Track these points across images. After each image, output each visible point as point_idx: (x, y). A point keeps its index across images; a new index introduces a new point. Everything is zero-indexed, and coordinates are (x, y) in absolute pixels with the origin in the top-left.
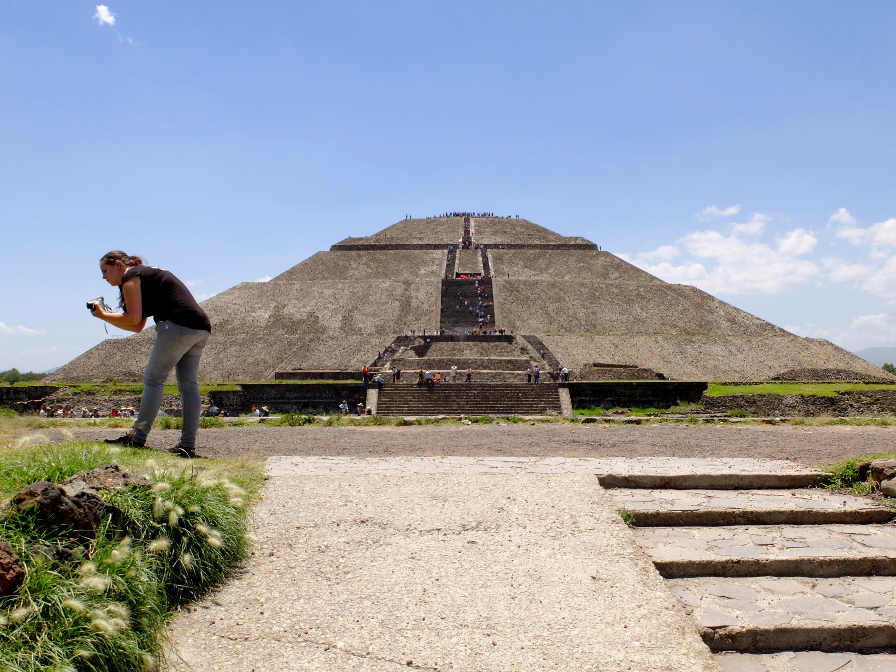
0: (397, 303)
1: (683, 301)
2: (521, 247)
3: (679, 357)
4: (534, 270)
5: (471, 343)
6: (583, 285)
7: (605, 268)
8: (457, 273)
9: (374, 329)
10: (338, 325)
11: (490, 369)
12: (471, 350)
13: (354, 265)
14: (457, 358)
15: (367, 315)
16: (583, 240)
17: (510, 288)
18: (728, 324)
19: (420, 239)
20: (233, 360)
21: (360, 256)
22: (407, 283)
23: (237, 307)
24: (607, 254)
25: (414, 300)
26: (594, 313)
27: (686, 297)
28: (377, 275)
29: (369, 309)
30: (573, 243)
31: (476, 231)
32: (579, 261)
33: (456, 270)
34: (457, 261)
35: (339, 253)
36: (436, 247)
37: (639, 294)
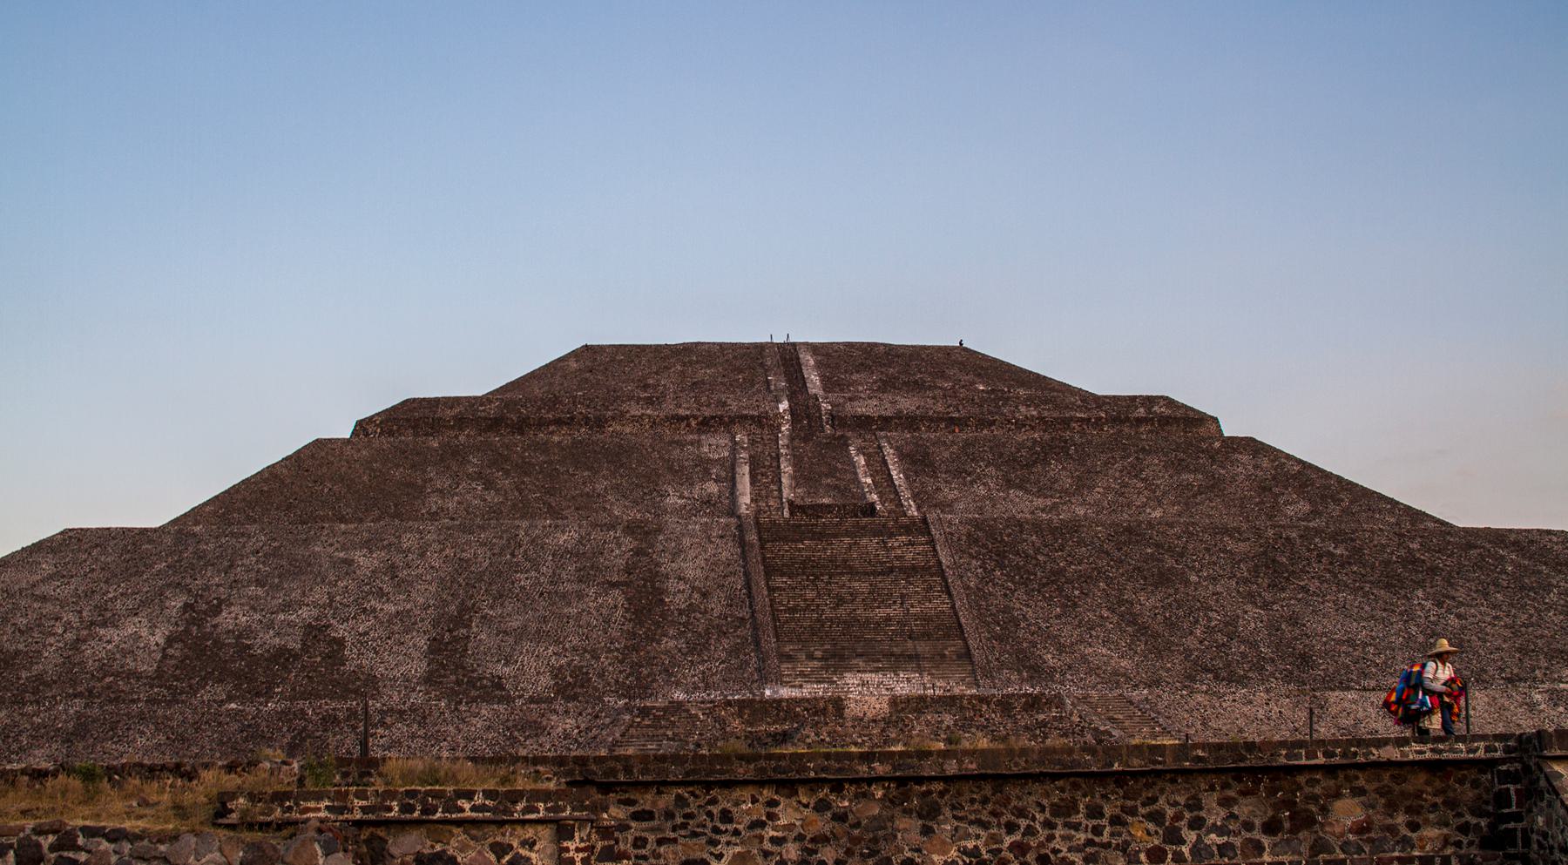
0: (617, 596)
2: (983, 423)
4: (1040, 493)
5: (948, 720)
6: (1226, 531)
7: (1264, 489)
8: (791, 503)
9: (546, 680)
10: (418, 667)
13: (443, 482)
15: (521, 634)
16: (1169, 402)
17: (992, 543)
19: (649, 401)
23: (49, 608)
24: (1252, 446)
25: (672, 585)
28: (524, 509)
31: (823, 378)
32: (1179, 466)
33: (787, 493)
34: (786, 468)
35: (385, 442)
36: (706, 425)
37: (1411, 561)
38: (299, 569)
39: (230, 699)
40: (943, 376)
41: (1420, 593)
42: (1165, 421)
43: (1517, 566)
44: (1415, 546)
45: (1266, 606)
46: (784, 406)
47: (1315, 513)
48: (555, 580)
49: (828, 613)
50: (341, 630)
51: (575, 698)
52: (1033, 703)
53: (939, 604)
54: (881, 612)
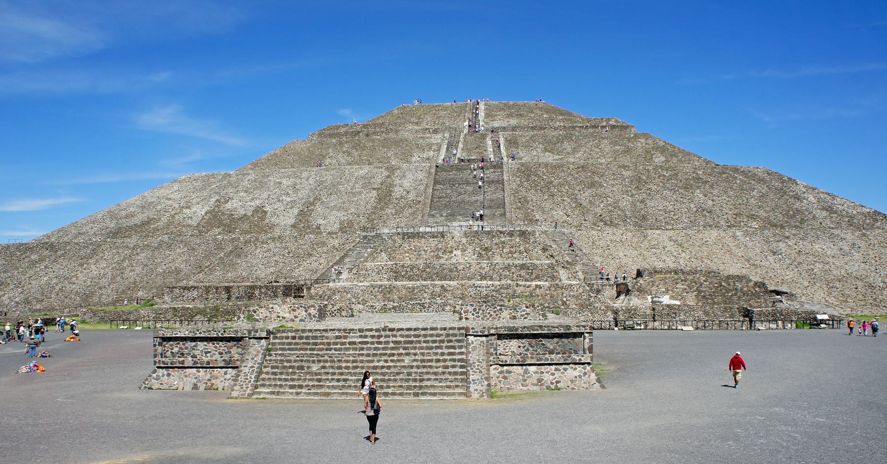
1: (758, 186)
2: (541, 128)
3: (771, 258)
6: (624, 167)
9: (337, 226)
10: (292, 221)
11: (491, 279)
12: (464, 250)
14: (442, 261)
17: (526, 172)
18: (825, 213)
19: (417, 123)
20: (138, 269)
21: (341, 144)
22: (392, 170)
23: (170, 202)
26: (642, 201)
27: (761, 180)
28: (360, 162)
29: (333, 201)
30: (604, 124)
32: (615, 143)
33: (458, 155)
34: (461, 145)
36: (436, 131)
37: (698, 179)
38: (261, 185)
39: (220, 234)
40: (532, 112)
41: (698, 191)
42: (613, 127)
43: (741, 181)
44: (700, 172)
45: (632, 196)
46: (467, 123)
47: (667, 161)
48: (353, 187)
49: (454, 199)
50: (268, 208)
51: (346, 232)
52: (523, 234)
53: (499, 195)
54: (474, 199)
